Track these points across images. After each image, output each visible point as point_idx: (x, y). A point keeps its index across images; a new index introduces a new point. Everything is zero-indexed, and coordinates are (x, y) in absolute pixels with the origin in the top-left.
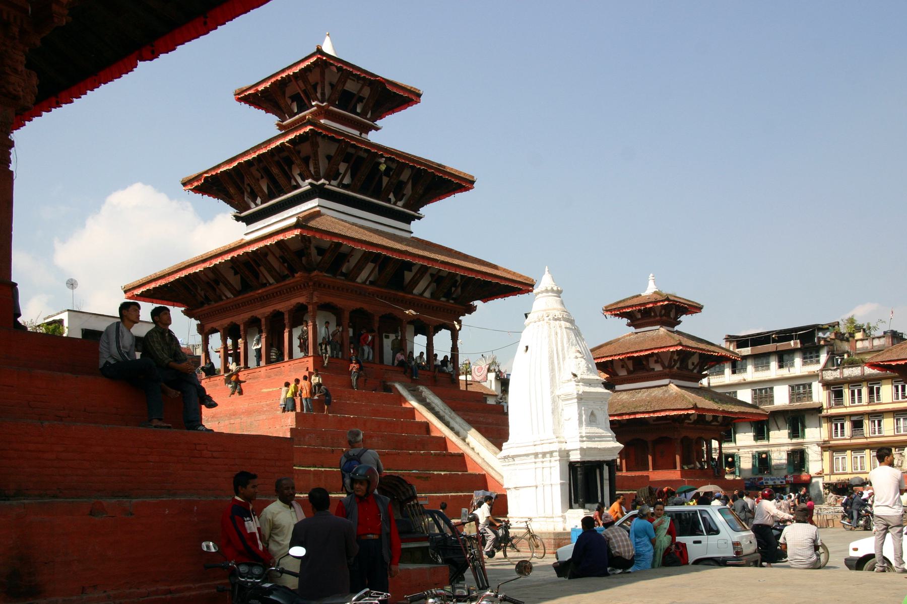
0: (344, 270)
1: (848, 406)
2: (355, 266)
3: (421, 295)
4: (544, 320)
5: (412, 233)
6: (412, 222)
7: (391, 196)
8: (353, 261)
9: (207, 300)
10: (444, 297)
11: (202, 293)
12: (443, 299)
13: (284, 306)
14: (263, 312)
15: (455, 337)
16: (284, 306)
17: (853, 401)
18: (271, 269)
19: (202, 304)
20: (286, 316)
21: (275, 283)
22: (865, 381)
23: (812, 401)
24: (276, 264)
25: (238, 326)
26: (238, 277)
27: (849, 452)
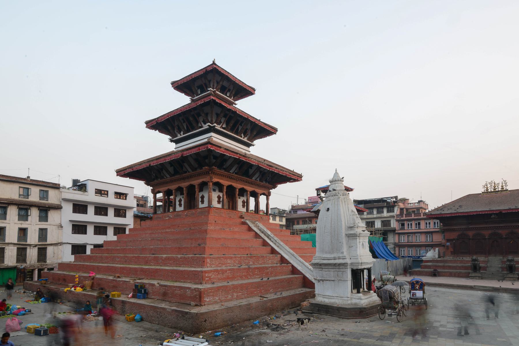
0: (224, 167)
1: (407, 229)
2: (229, 165)
3: (256, 180)
4: (337, 195)
5: (250, 152)
6: (250, 147)
7: (242, 135)
8: (229, 163)
9: (157, 178)
10: (264, 181)
11: (154, 175)
12: (264, 182)
13: (196, 182)
14: (184, 185)
15: (268, 199)
16: (196, 182)
17: (409, 228)
18: (190, 165)
19: (154, 180)
20: (196, 187)
21: (191, 171)
22: (406, 220)
23: (391, 226)
24: (192, 162)
25: (172, 191)
26: (172, 167)
27: (406, 248)
